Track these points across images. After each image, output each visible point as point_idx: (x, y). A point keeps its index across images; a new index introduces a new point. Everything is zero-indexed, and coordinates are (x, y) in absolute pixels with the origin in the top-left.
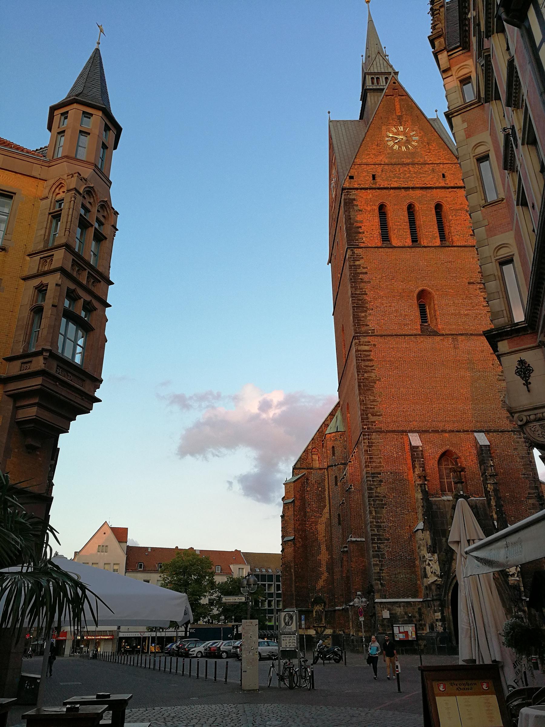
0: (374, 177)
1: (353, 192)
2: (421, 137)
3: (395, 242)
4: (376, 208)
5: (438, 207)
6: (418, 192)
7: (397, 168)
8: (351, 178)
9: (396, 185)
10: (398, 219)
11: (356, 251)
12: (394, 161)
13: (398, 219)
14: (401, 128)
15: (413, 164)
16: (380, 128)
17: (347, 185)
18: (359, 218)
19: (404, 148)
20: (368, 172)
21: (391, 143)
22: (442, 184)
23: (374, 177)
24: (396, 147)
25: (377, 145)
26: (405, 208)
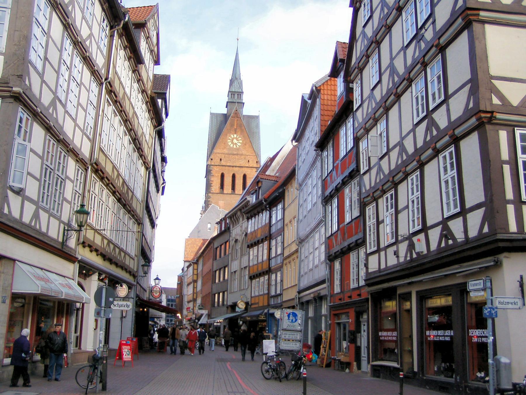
0: (221, 159)
1: (212, 167)
2: (243, 141)
3: (225, 192)
4: (220, 175)
5: (245, 177)
6: (237, 168)
7: (231, 156)
8: (212, 159)
9: (228, 164)
10: (228, 180)
11: (209, 194)
12: (230, 152)
13: (228, 180)
14: (235, 136)
15: (237, 155)
16: (226, 135)
17: (209, 163)
18: (212, 179)
19: (235, 146)
20: (218, 157)
21: (230, 143)
22: (247, 166)
23: (221, 159)
24: (232, 145)
25: (224, 144)
26: (231, 175)
